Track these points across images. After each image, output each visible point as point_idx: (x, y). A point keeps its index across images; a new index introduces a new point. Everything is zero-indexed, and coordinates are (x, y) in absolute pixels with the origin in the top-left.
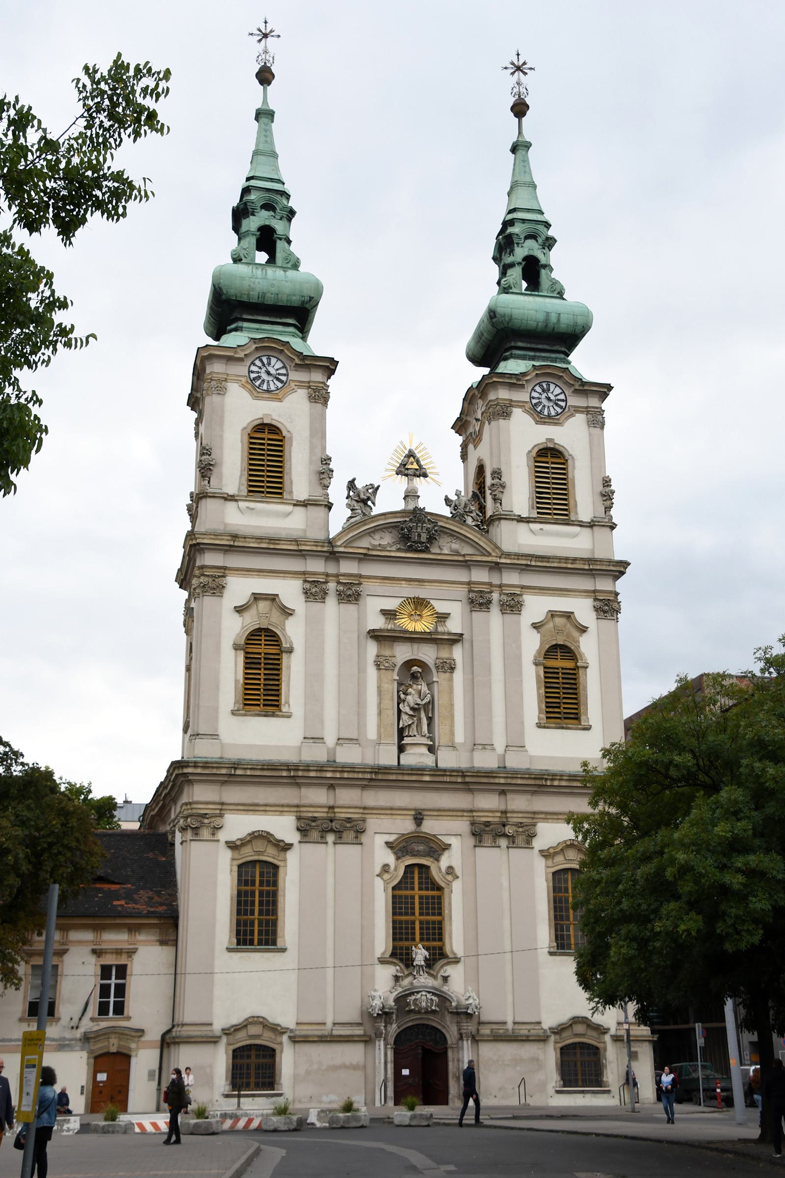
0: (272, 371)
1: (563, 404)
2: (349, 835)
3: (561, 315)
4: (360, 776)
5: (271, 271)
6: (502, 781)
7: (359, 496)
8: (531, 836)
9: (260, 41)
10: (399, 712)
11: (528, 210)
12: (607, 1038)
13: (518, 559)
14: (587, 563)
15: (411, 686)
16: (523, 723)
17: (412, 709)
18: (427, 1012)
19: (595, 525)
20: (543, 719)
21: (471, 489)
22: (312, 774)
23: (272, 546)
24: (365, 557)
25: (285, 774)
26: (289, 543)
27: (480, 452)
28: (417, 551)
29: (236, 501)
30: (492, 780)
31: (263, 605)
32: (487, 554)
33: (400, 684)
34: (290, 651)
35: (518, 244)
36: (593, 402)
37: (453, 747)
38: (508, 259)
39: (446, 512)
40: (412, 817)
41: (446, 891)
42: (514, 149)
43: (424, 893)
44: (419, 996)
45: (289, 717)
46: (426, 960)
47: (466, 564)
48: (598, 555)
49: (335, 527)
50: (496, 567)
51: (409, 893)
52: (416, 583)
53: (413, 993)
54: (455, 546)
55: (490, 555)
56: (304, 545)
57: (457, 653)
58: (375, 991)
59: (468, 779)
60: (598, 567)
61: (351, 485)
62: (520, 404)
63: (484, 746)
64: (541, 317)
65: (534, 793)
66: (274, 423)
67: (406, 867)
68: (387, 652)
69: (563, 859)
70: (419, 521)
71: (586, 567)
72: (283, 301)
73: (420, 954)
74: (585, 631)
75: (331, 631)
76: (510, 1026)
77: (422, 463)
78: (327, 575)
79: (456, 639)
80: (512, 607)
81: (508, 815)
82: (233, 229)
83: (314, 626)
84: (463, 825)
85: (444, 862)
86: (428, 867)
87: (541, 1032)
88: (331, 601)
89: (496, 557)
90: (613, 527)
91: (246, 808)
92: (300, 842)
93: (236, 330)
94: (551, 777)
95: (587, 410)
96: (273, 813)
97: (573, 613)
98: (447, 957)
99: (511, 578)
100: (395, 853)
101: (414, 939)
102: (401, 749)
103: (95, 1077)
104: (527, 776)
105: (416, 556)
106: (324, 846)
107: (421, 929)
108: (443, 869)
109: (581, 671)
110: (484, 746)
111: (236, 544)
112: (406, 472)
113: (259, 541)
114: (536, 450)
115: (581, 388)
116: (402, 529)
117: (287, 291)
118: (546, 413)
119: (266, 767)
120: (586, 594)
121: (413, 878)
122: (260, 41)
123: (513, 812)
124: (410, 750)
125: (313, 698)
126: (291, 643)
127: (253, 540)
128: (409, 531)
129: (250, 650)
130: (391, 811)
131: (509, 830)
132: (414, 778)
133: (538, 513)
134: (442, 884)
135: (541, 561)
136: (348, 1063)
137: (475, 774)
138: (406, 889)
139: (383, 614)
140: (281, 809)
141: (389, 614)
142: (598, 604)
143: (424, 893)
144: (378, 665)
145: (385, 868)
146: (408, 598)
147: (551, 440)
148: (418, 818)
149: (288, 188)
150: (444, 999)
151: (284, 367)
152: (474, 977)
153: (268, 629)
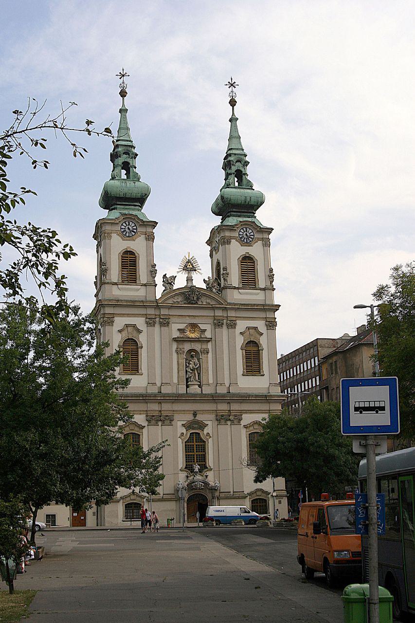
0: (131, 228)
1: (252, 237)
4: (171, 398)
5: (128, 183)
6: (229, 398)
7: (168, 281)
8: (240, 420)
9: (120, 78)
10: (186, 371)
11: (237, 149)
12: (269, 496)
15: (191, 361)
17: (191, 370)
18: (200, 489)
21: (215, 277)
22: (152, 398)
27: (218, 256)
28: (192, 304)
29: (118, 285)
31: (129, 328)
33: (186, 360)
35: (233, 164)
36: (265, 236)
38: (229, 172)
39: (204, 286)
41: (206, 442)
42: (230, 120)
44: (196, 483)
46: (199, 469)
47: (213, 308)
48: (267, 303)
49: (158, 296)
53: (194, 482)
54: (209, 301)
58: (179, 482)
61: (165, 276)
62: (234, 238)
63: (221, 384)
64: (243, 198)
66: (131, 250)
67: (191, 434)
68: (181, 347)
71: (263, 308)
72: (134, 196)
73: (197, 468)
76: (232, 493)
77: (194, 265)
78: (156, 315)
79: (208, 341)
82: (111, 160)
83: (150, 337)
84: (213, 416)
85: (206, 431)
87: (244, 495)
88: (157, 326)
90: (274, 289)
93: (114, 209)
95: (262, 239)
97: (257, 327)
98: (207, 468)
99: (232, 314)
100: (186, 428)
101: (194, 462)
102: (187, 386)
103: (73, 514)
106: (157, 426)
108: (205, 434)
110: (221, 384)
114: (242, 257)
117: (135, 192)
118: (245, 241)
122: (120, 78)
124: (192, 387)
125: (151, 367)
126: (142, 344)
129: (125, 348)
131: (232, 418)
132: (193, 398)
133: (243, 285)
134: (205, 440)
136: (169, 509)
143: (197, 443)
144: (177, 352)
148: (195, 415)
149: (134, 143)
150: (206, 484)
151: (135, 226)
152: (218, 477)
153: (132, 339)
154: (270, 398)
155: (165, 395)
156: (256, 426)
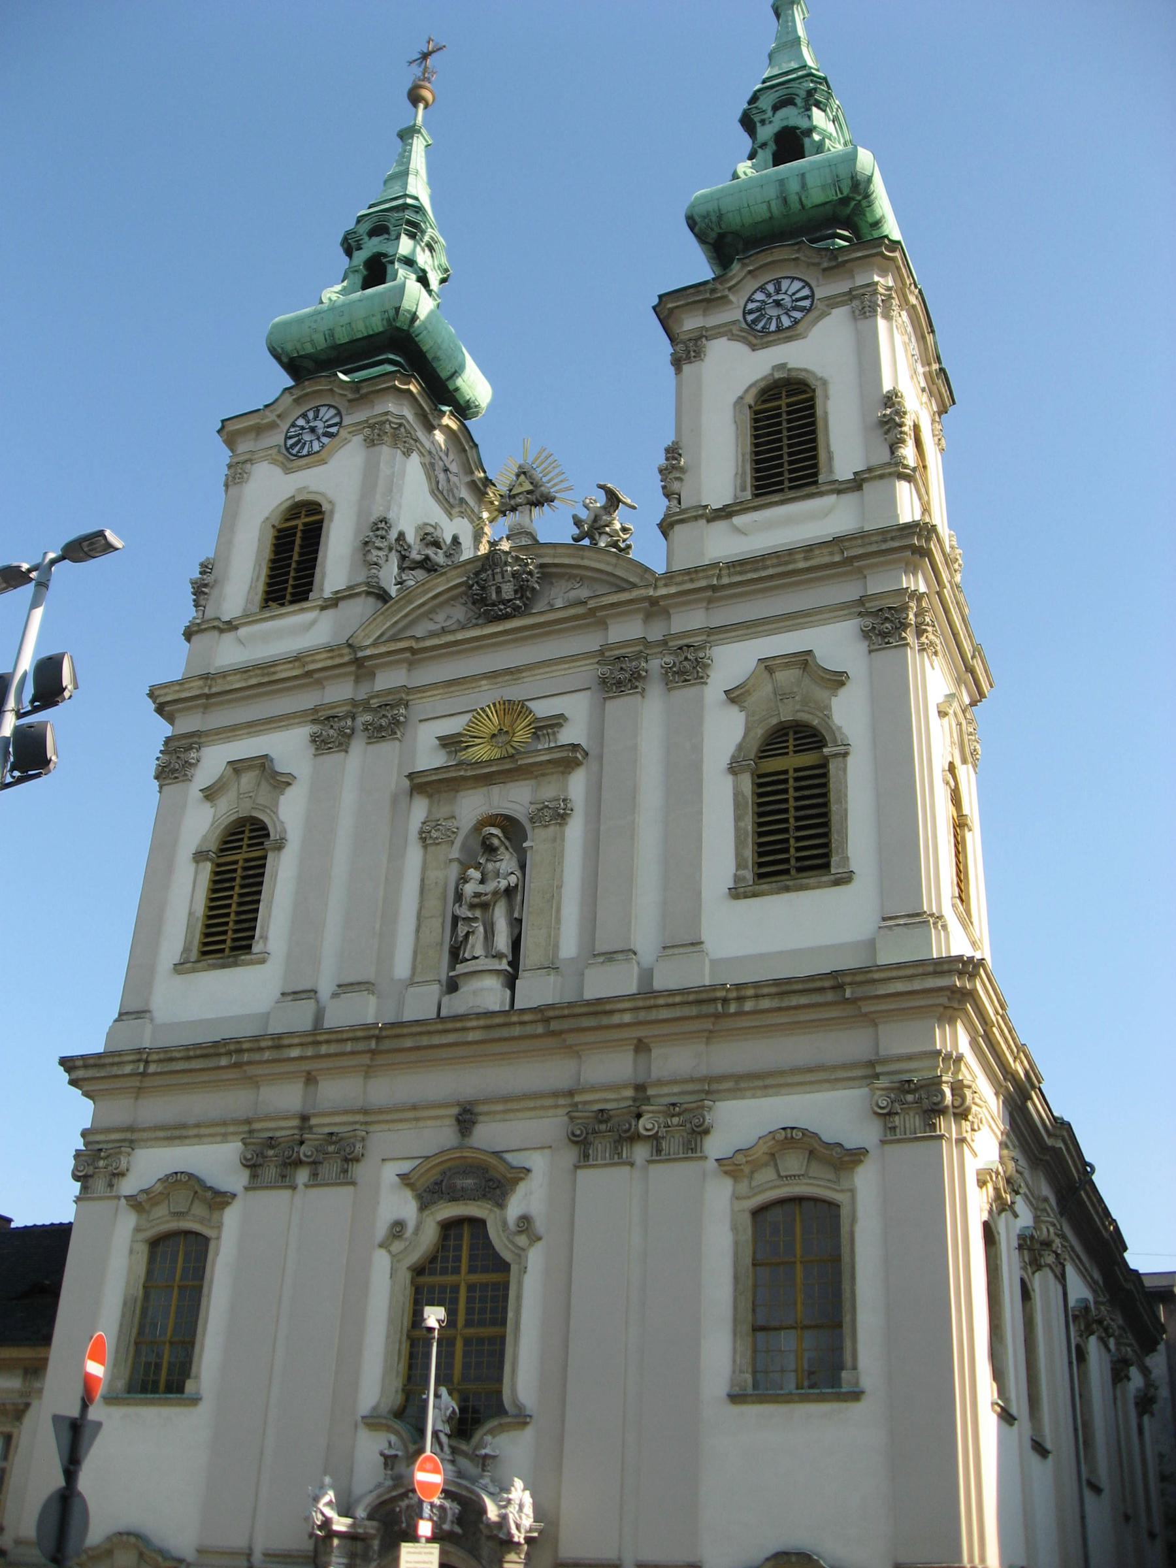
2: (330, 1169)
3: (807, 176)
4: (349, 1047)
6: (627, 1018)
8: (700, 1131)
13: (692, 580)
14: (836, 549)
16: (698, 894)
19: (864, 480)
20: (744, 879)
23: (266, 679)
24: (415, 656)
25: (224, 1061)
26: (290, 666)
30: (605, 1021)
31: (248, 779)
32: (625, 585)
34: (280, 846)
37: (552, 967)
40: (453, 1121)
41: (514, 1268)
43: (475, 1278)
45: (263, 961)
50: (655, 609)
51: (449, 1279)
52: (507, 678)
55: (634, 586)
56: (314, 661)
57: (577, 785)
59: (554, 1025)
60: (860, 551)
63: (610, 956)
65: (710, 1036)
68: (443, 811)
69: (772, 1176)
70: (496, 565)
71: (837, 558)
72: (361, 330)
74: (842, 684)
75: (349, 797)
80: (684, 673)
81: (650, 1092)
85: (515, 1207)
86: (478, 1224)
89: (646, 586)
91: (169, 1134)
92: (247, 1189)
94: (734, 994)
96: (210, 1139)
100: (419, 1197)
104: (678, 999)
105: (500, 628)
107: (466, 1354)
109: (833, 766)
110: (610, 956)
111: (214, 690)
112: (513, 502)
113: (245, 676)
114: (754, 391)
115: (834, 263)
116: (471, 587)
119: (191, 1053)
120: (845, 612)
121: (458, 1248)
123: (660, 1083)
127: (238, 676)
128: (483, 588)
130: (414, 1111)
134: (507, 1256)
135: (741, 573)
137: (566, 1012)
138: (444, 1271)
139: (444, 746)
140: (222, 1130)
141: (449, 743)
142: (868, 621)
143: (475, 1278)
145: (397, 1229)
146: (482, 709)
147: (782, 366)
148: (466, 1119)
154: (860, 991)
155: (339, 1036)
156: (793, 1163)
